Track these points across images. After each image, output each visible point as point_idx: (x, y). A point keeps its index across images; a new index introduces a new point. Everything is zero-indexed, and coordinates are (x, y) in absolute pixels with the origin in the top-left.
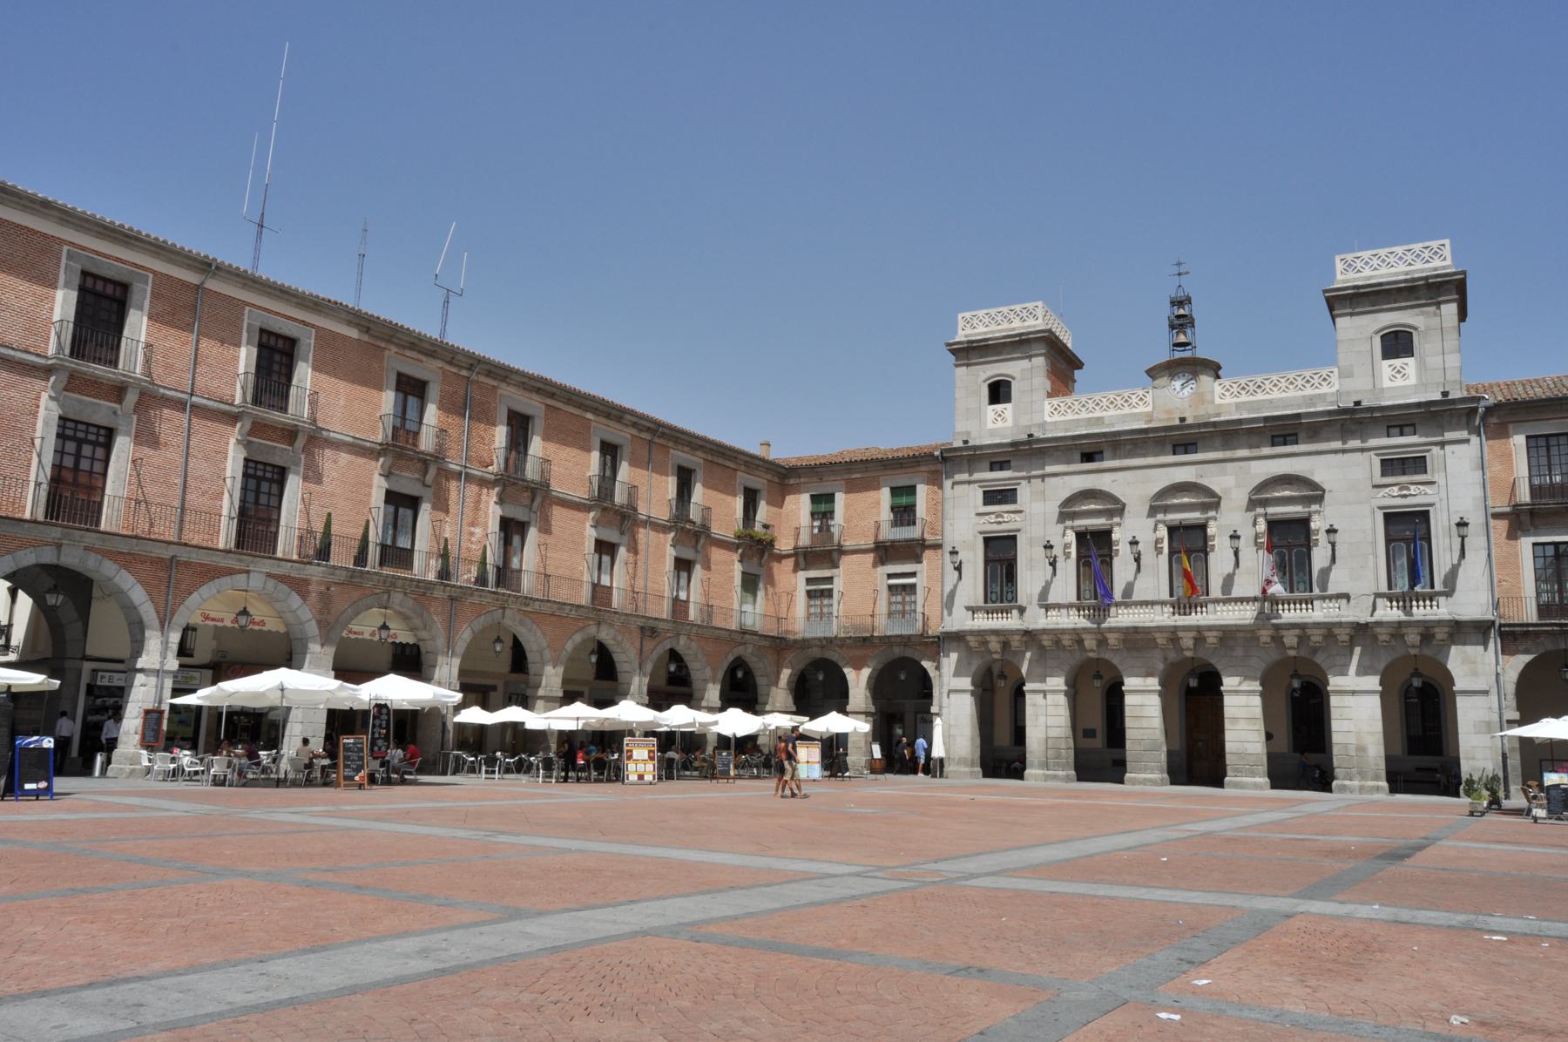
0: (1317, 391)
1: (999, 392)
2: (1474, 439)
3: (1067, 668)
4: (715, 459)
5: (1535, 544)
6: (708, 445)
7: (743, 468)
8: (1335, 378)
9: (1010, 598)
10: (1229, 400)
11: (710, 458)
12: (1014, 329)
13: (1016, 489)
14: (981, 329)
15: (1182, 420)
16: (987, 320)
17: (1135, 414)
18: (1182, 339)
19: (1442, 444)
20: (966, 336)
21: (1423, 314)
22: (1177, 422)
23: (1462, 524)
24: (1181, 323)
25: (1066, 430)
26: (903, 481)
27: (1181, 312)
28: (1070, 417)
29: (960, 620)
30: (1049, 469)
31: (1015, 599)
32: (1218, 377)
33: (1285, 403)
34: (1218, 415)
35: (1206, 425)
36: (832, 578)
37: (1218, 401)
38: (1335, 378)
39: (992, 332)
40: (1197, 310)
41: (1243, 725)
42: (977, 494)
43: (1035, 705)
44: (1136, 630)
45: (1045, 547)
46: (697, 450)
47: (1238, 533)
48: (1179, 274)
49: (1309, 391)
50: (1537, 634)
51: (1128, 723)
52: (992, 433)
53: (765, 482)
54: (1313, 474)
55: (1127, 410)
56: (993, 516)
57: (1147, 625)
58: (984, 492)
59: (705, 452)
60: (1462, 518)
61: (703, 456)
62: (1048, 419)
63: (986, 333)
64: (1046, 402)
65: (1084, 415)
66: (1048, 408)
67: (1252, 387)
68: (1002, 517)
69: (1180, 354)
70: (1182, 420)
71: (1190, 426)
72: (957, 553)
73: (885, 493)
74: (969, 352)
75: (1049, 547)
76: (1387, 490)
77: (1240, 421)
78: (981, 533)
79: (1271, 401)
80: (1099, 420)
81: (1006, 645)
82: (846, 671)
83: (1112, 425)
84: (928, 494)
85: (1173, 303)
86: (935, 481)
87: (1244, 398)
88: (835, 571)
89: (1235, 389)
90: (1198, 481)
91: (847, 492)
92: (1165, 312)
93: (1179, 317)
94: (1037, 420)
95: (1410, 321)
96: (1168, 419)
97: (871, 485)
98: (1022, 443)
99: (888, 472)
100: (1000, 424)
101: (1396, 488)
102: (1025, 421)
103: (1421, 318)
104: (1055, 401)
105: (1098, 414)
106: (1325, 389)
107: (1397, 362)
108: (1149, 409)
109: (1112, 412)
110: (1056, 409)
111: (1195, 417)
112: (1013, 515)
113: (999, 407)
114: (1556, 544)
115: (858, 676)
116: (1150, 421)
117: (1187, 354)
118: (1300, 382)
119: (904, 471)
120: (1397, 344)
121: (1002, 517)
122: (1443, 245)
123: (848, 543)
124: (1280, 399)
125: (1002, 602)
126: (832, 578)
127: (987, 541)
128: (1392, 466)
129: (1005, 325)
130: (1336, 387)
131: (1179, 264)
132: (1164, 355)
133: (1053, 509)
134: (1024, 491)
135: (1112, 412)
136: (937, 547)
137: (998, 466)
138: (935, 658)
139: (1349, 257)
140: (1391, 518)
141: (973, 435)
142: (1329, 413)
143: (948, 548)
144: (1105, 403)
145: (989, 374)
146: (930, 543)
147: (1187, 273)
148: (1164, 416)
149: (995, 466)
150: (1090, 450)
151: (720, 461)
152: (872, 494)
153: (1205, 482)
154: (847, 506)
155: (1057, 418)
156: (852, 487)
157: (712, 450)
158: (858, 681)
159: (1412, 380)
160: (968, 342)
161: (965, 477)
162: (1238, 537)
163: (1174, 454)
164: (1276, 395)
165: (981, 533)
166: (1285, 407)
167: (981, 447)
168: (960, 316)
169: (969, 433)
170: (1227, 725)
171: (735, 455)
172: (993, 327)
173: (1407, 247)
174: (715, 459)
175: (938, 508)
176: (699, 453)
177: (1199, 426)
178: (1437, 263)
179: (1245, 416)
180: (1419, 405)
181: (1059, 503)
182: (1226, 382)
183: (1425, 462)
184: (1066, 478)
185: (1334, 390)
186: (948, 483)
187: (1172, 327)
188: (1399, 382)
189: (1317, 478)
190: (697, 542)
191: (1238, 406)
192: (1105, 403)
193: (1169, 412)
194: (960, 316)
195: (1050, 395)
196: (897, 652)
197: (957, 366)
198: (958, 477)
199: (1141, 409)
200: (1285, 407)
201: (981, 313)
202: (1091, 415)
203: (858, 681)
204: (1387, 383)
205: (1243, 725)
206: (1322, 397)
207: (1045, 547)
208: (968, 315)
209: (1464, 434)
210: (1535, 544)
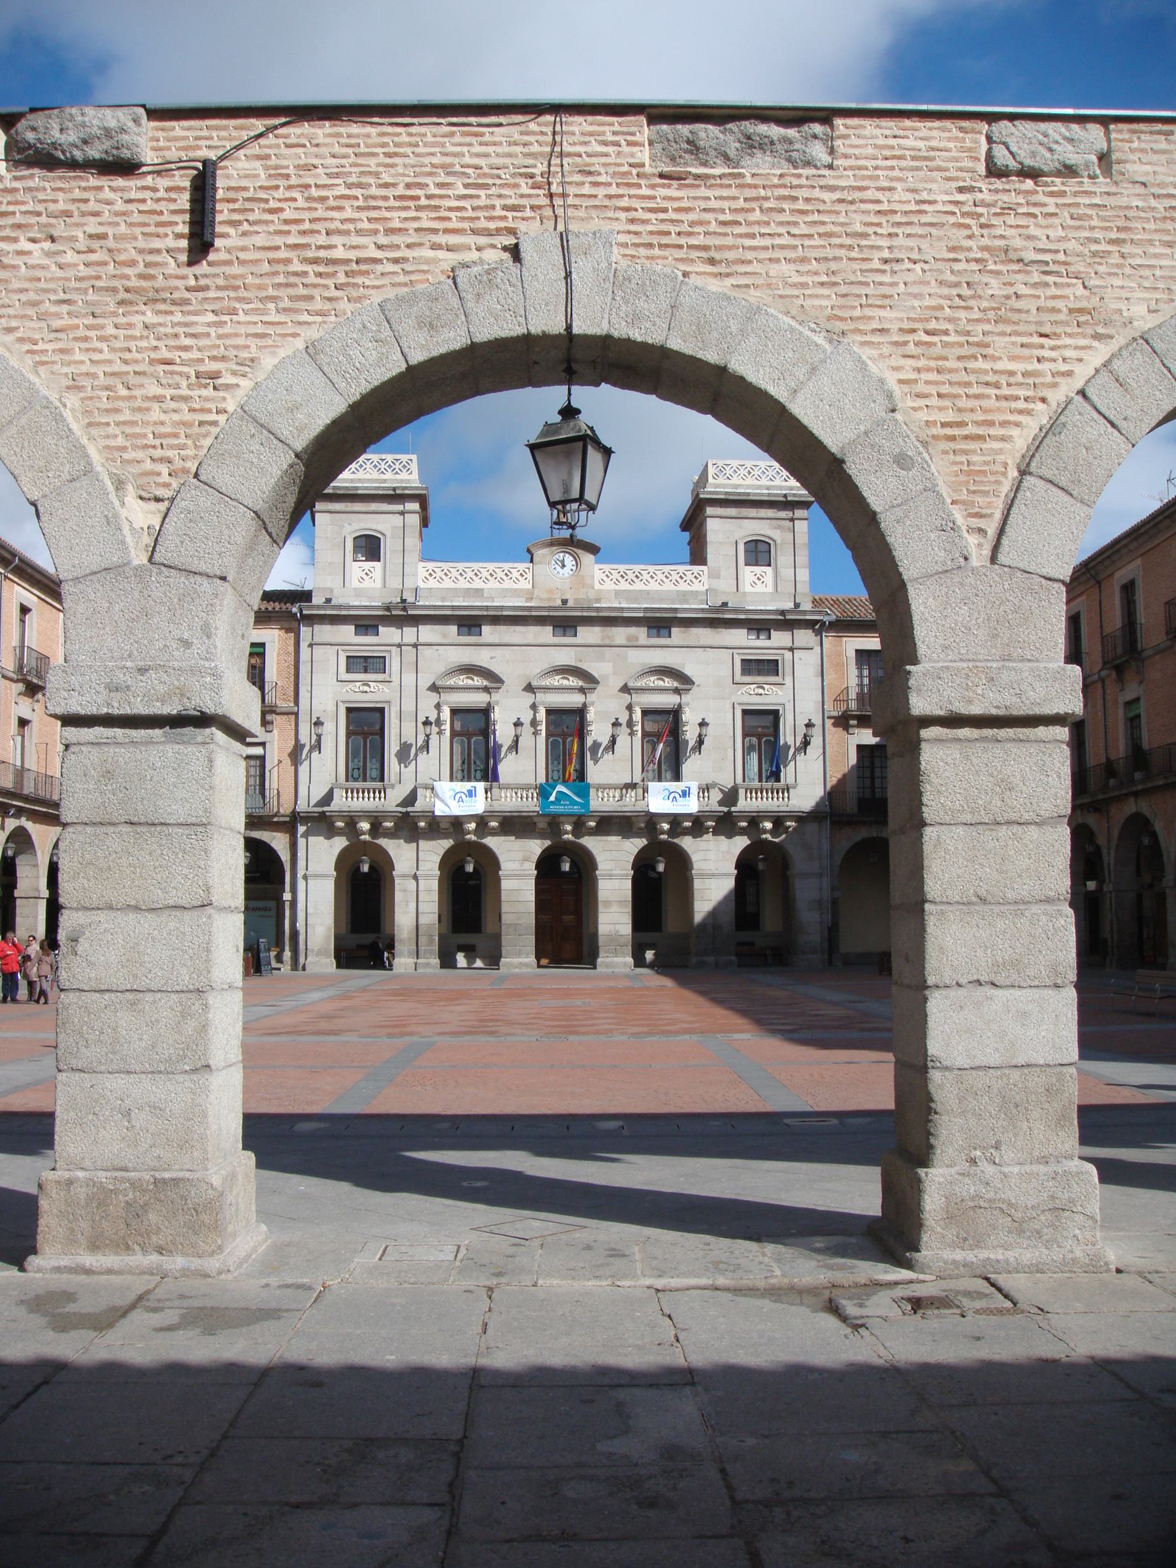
8: (704, 578)
10: (609, 586)
12: (385, 481)
15: (565, 602)
17: (516, 590)
21: (779, 527)
22: (559, 603)
25: (443, 600)
33: (660, 596)
34: (598, 600)
35: (590, 609)
37: (597, 586)
38: (704, 578)
39: (360, 480)
41: (615, 908)
43: (404, 891)
51: (505, 908)
52: (358, 593)
55: (508, 584)
58: (348, 657)
62: (422, 585)
63: (352, 481)
64: (421, 564)
65: (463, 584)
67: (631, 576)
70: (565, 602)
71: (572, 609)
78: (343, 702)
79: (648, 592)
80: (478, 592)
83: (492, 599)
84: (279, 655)
87: (624, 586)
94: (409, 584)
96: (549, 599)
98: (396, 608)
100: (368, 583)
102: (395, 583)
103: (779, 531)
105: (477, 584)
107: (758, 570)
109: (493, 584)
111: (575, 600)
112: (381, 686)
116: (531, 599)
125: (365, 780)
127: (349, 710)
129: (375, 475)
130: (706, 587)
133: (425, 681)
141: (336, 593)
142: (703, 610)
145: (355, 526)
146: (283, 710)
148: (544, 595)
153: (584, 666)
155: (432, 583)
159: (770, 588)
164: (653, 586)
165: (343, 702)
166: (661, 600)
169: (332, 590)
170: (601, 909)
183: (777, 666)
188: (760, 588)
189: (688, 672)
191: (618, 594)
193: (550, 591)
200: (661, 600)
204: (748, 588)
205: (615, 908)
206: (695, 594)
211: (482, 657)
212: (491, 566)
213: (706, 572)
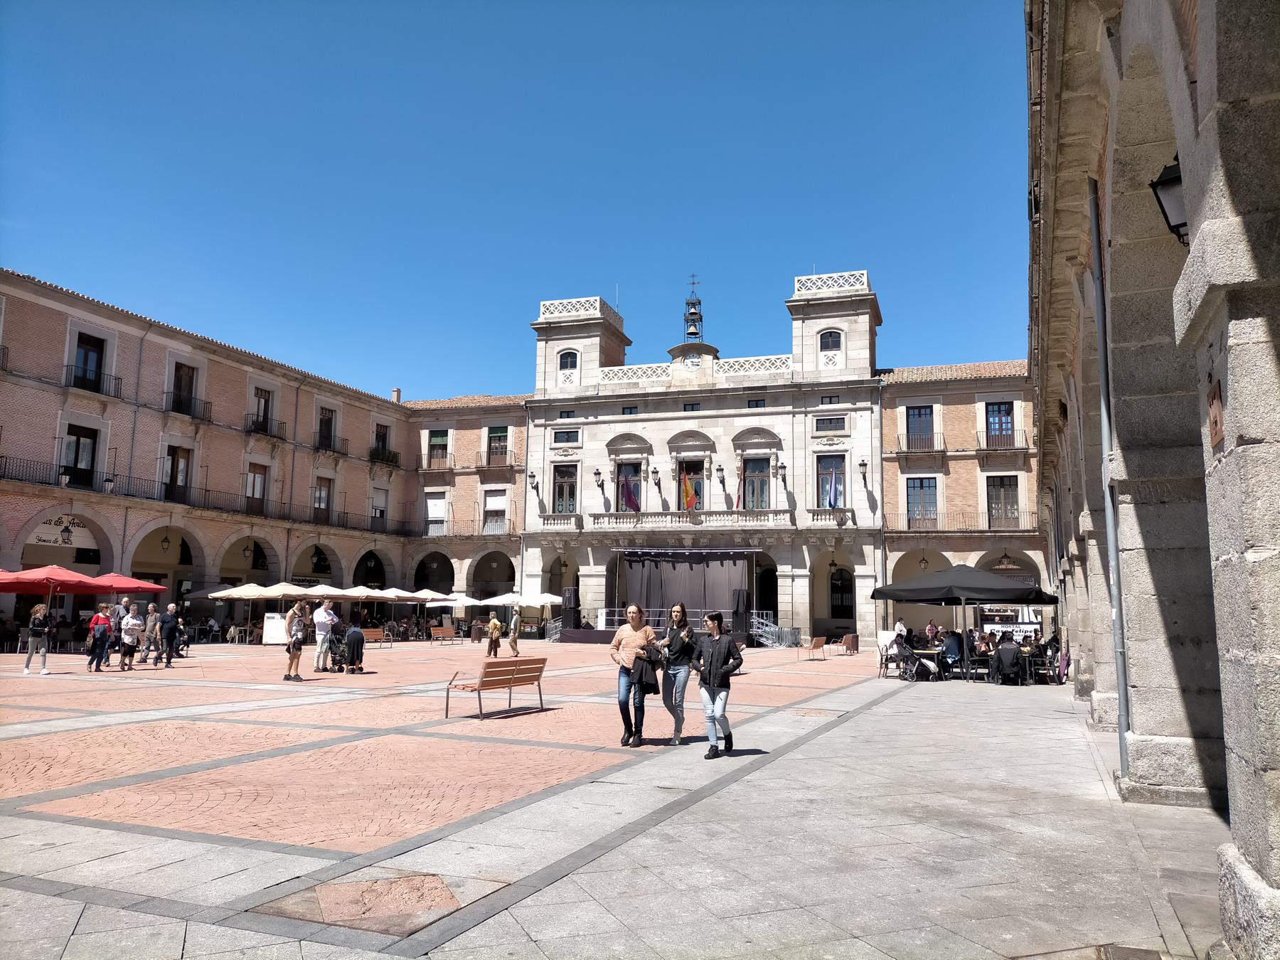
0: (779, 371)
1: (568, 360)
2: (876, 408)
3: (609, 559)
4: (352, 402)
5: (908, 479)
6: (346, 392)
7: (376, 409)
8: (790, 361)
9: (571, 509)
11: (348, 401)
12: (579, 316)
13: (577, 432)
14: (556, 314)
16: (560, 308)
18: (692, 329)
19: (855, 410)
20: (545, 319)
23: (863, 465)
24: (695, 319)
26: (498, 423)
27: (693, 310)
28: (616, 381)
29: (534, 523)
30: (601, 418)
31: (574, 510)
32: (718, 359)
35: (706, 391)
36: (444, 492)
40: (704, 310)
42: (550, 434)
44: (653, 532)
45: (595, 474)
46: (337, 395)
47: (722, 467)
48: (694, 283)
49: (773, 371)
50: (906, 538)
53: (395, 420)
54: (773, 428)
56: (561, 451)
57: (662, 529)
59: (342, 397)
60: (863, 461)
61: (343, 400)
63: (559, 317)
65: (625, 380)
66: (601, 375)
68: (568, 451)
69: (693, 341)
72: (534, 476)
73: (485, 431)
74: (549, 331)
75: (598, 474)
76: (819, 440)
77: (727, 390)
80: (636, 384)
81: (566, 543)
82: (452, 561)
85: (688, 304)
86: (521, 423)
88: (448, 488)
89: (726, 367)
90: (700, 430)
91: (457, 429)
92: (682, 310)
93: (692, 314)
95: (839, 325)
97: (477, 426)
99: (486, 416)
101: (825, 439)
104: (606, 369)
105: (634, 380)
106: (783, 370)
107: (830, 353)
108: (670, 378)
110: (606, 375)
113: (567, 372)
114: (922, 479)
115: (461, 565)
117: (697, 341)
118: (768, 364)
119: (499, 415)
120: (830, 340)
121: (568, 451)
122: (863, 274)
123: (458, 468)
124: (755, 376)
126: (444, 492)
128: (823, 424)
129: (574, 313)
131: (693, 276)
132: (680, 341)
134: (584, 434)
135: (644, 379)
136: (521, 471)
137: (566, 414)
138: (517, 552)
139: (803, 278)
140: (821, 459)
143: (529, 473)
144: (640, 373)
147: (699, 283)
149: (563, 414)
150: (630, 405)
151: (357, 404)
152: (476, 431)
154: (457, 440)
156: (461, 426)
157: (349, 395)
158: (462, 569)
160: (547, 323)
161: (542, 421)
162: (722, 470)
163: (685, 411)
164: (752, 372)
165: (552, 462)
167: (554, 401)
168: (542, 303)
171: (369, 399)
172: (565, 314)
173: (840, 274)
174: (352, 402)
175: (525, 444)
176: (339, 398)
177: (701, 392)
178: (858, 286)
179: (732, 386)
180: (842, 383)
181: (606, 442)
182: (721, 361)
184: (612, 425)
185: (790, 371)
186: (531, 426)
187: (687, 321)
190: (336, 465)
191: (727, 379)
192: (640, 373)
193: (682, 381)
194: (542, 303)
195: (603, 364)
196: (491, 548)
197: (539, 340)
198: (538, 422)
199: (664, 378)
201: (556, 302)
202: (630, 381)
203: (462, 569)
207: (595, 474)
208: (548, 303)
209: (868, 404)
210: (908, 479)
211: (636, 429)
212: (644, 367)
213: (791, 359)
